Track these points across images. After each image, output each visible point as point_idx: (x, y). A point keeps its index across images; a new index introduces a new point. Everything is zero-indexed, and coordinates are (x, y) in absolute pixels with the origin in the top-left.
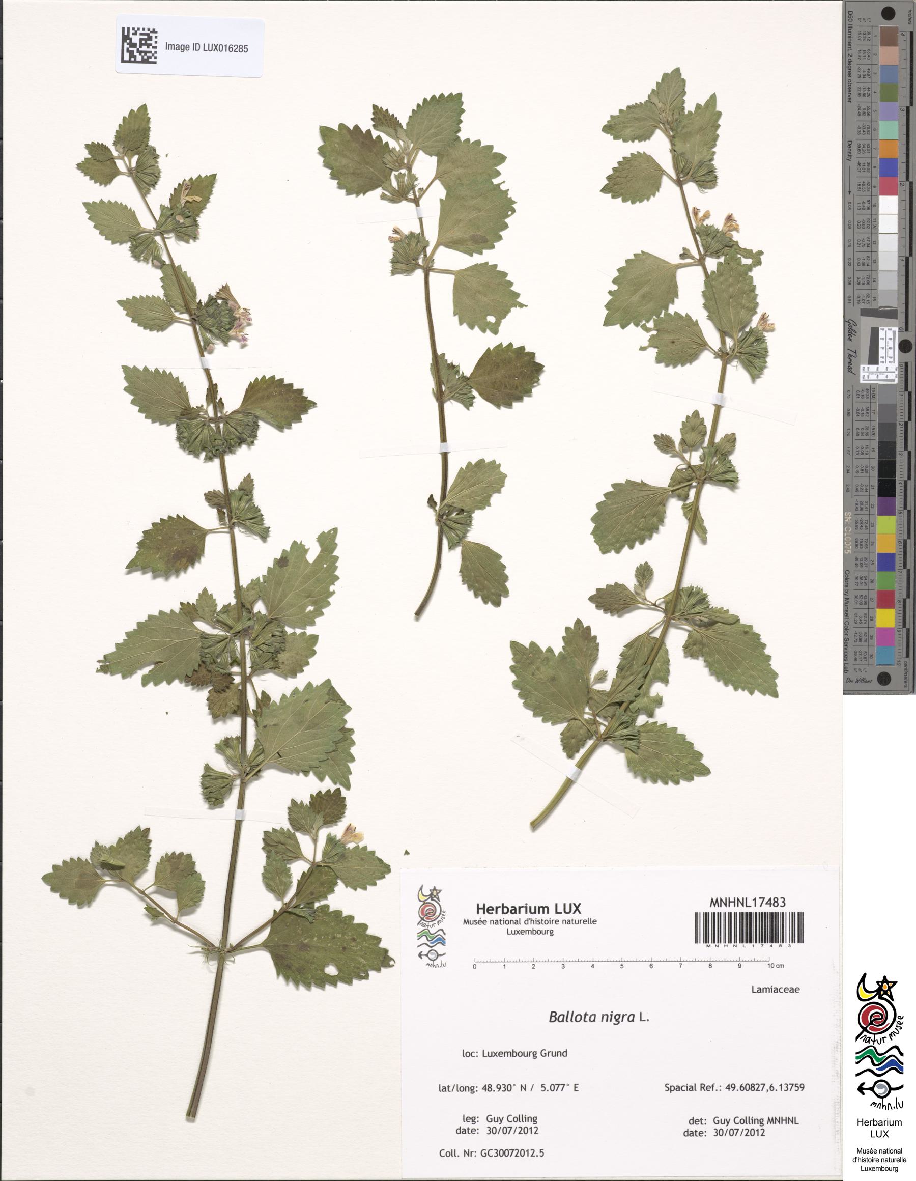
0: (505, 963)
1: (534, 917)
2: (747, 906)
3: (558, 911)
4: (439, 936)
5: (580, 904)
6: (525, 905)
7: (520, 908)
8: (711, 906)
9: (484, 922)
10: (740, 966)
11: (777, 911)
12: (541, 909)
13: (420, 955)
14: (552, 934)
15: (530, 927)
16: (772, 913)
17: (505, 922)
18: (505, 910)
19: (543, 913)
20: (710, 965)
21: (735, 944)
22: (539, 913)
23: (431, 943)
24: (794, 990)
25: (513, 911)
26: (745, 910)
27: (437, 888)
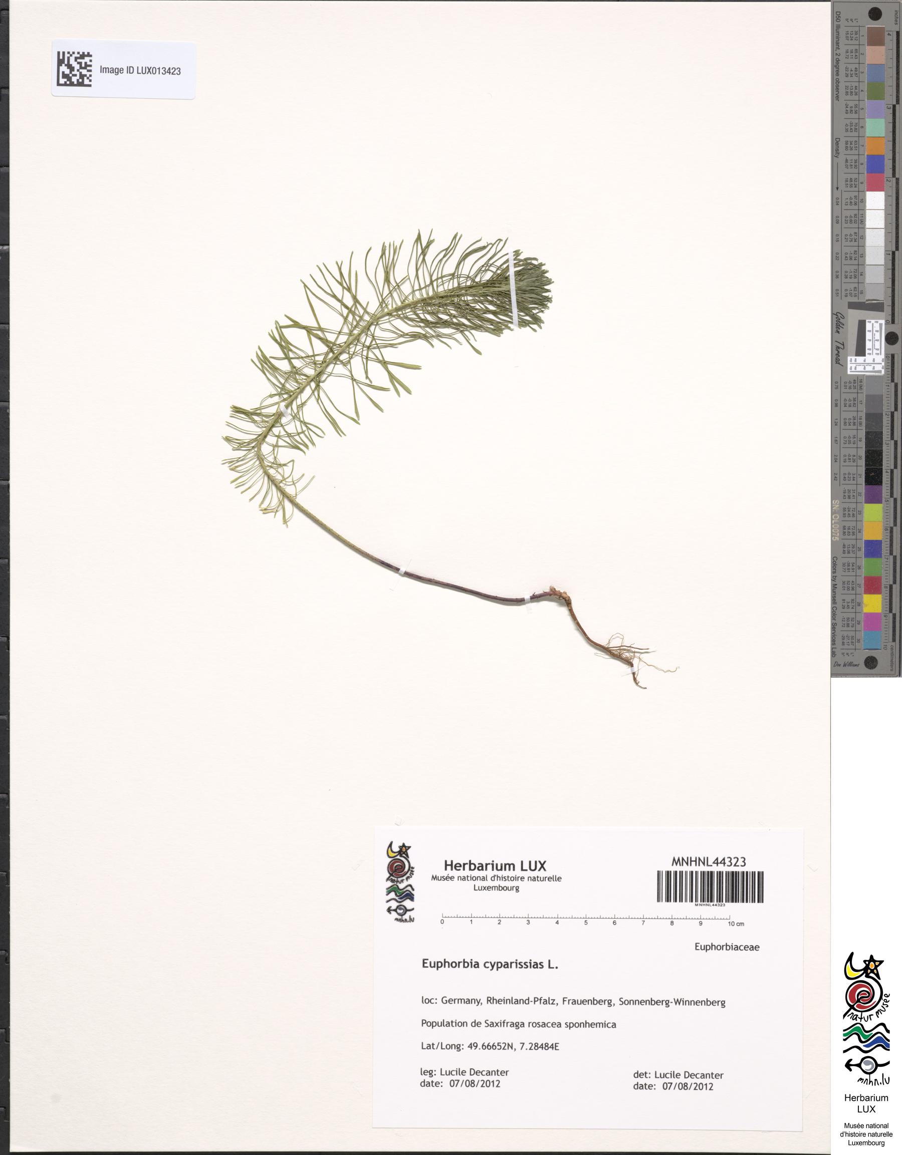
0: (471, 918)
1: (500, 873)
3: (524, 868)
4: (407, 892)
5: (545, 862)
6: (491, 862)
9: (452, 878)
10: (701, 924)
12: (507, 866)
13: (389, 910)
14: (517, 890)
16: (733, 872)
17: (472, 878)
18: (473, 867)
19: (510, 870)
20: (672, 923)
21: (697, 903)
22: (505, 870)
23: (400, 899)
24: (754, 948)
26: (706, 869)
27: (406, 845)
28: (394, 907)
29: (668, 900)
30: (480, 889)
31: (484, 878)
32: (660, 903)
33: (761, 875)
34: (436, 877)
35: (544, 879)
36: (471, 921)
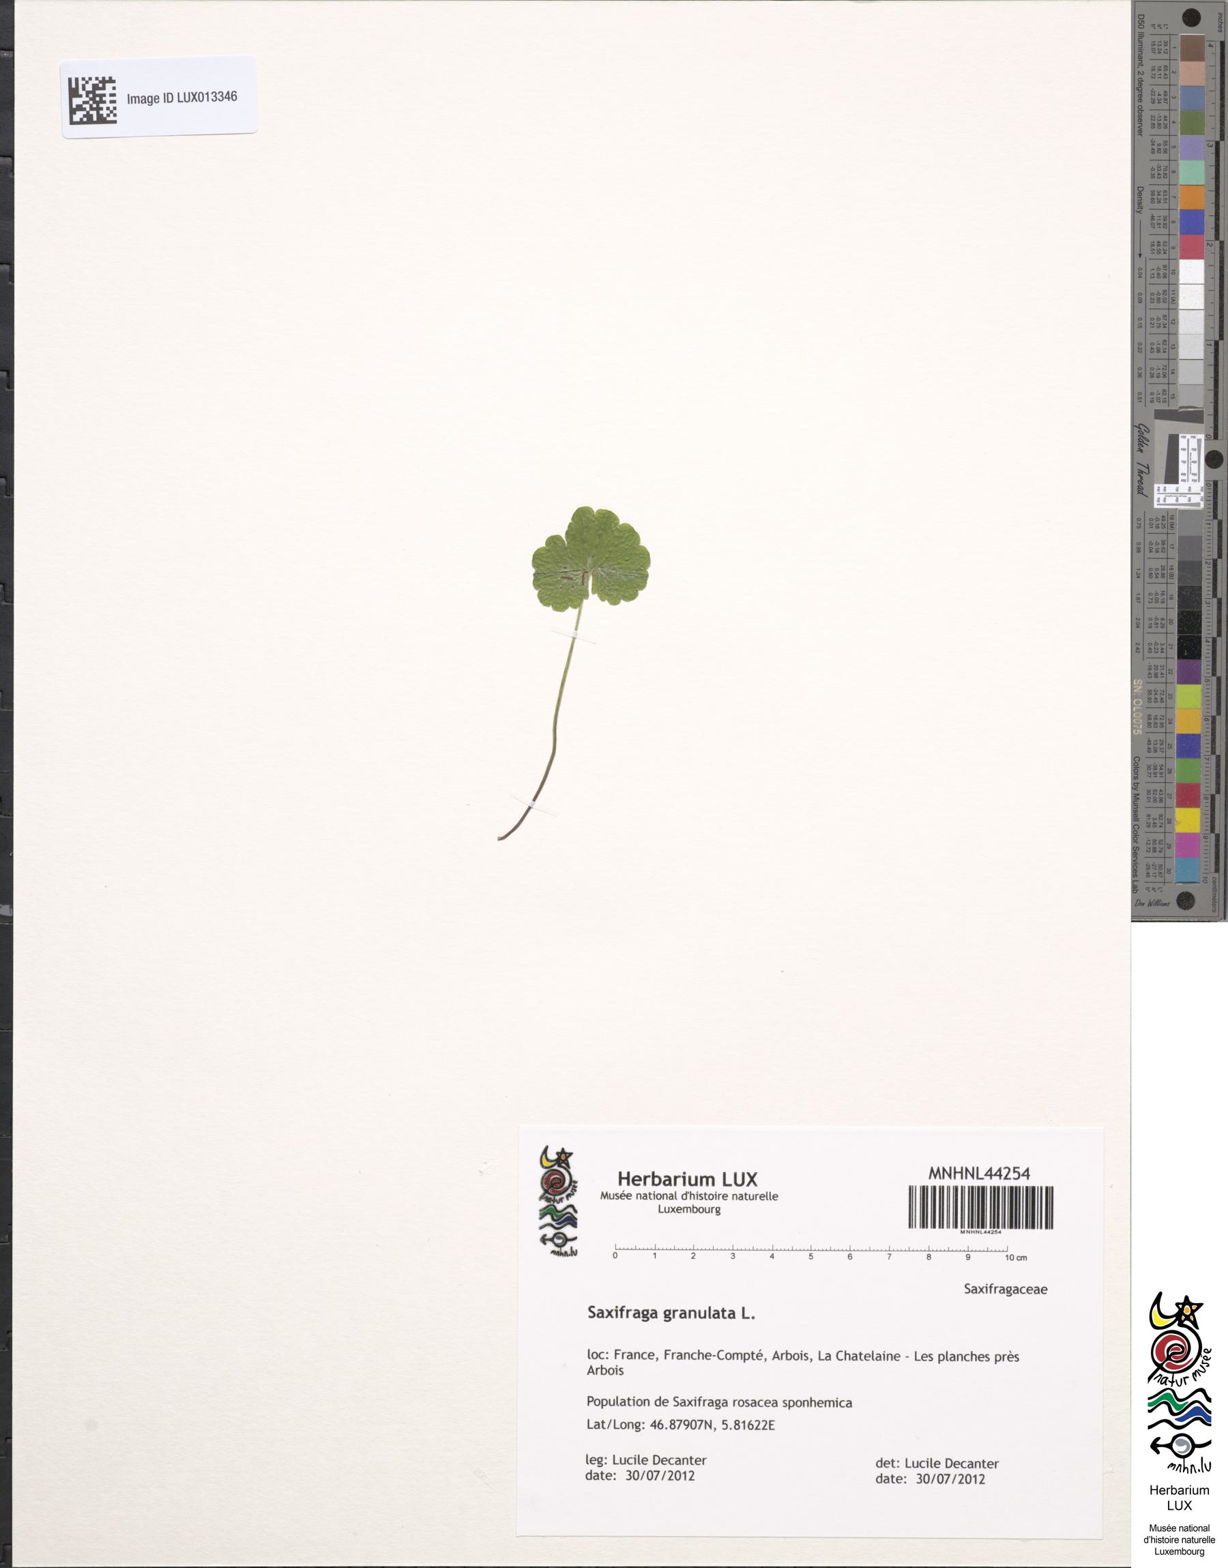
0: (655, 1251)
1: (694, 1190)
2: (978, 1178)
3: (727, 1183)
5: (755, 1174)
6: (682, 1175)
7: (676, 1178)
8: (930, 1178)
9: (628, 1196)
10: (968, 1258)
11: (1018, 1185)
12: (704, 1180)
13: (544, 1240)
14: (718, 1213)
15: (689, 1203)
16: (1012, 1188)
17: (656, 1197)
18: (657, 1181)
19: (707, 1184)
20: (929, 1256)
21: (963, 1230)
22: (701, 1184)
23: (557, 1224)
24: (1041, 1290)
25: (667, 1183)
26: (976, 1183)
27: (567, 1150)
28: (550, 1235)
29: (924, 1225)
30: (667, 1211)
31: (672, 1196)
32: (913, 1230)
33: (1049, 1191)
34: (607, 1194)
35: (754, 1197)
36: (655, 1254)
